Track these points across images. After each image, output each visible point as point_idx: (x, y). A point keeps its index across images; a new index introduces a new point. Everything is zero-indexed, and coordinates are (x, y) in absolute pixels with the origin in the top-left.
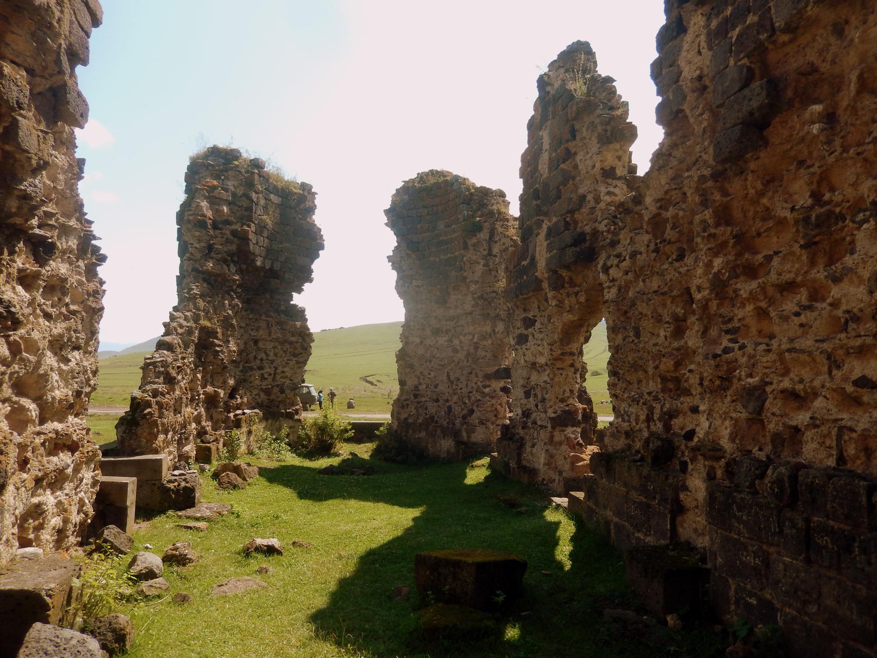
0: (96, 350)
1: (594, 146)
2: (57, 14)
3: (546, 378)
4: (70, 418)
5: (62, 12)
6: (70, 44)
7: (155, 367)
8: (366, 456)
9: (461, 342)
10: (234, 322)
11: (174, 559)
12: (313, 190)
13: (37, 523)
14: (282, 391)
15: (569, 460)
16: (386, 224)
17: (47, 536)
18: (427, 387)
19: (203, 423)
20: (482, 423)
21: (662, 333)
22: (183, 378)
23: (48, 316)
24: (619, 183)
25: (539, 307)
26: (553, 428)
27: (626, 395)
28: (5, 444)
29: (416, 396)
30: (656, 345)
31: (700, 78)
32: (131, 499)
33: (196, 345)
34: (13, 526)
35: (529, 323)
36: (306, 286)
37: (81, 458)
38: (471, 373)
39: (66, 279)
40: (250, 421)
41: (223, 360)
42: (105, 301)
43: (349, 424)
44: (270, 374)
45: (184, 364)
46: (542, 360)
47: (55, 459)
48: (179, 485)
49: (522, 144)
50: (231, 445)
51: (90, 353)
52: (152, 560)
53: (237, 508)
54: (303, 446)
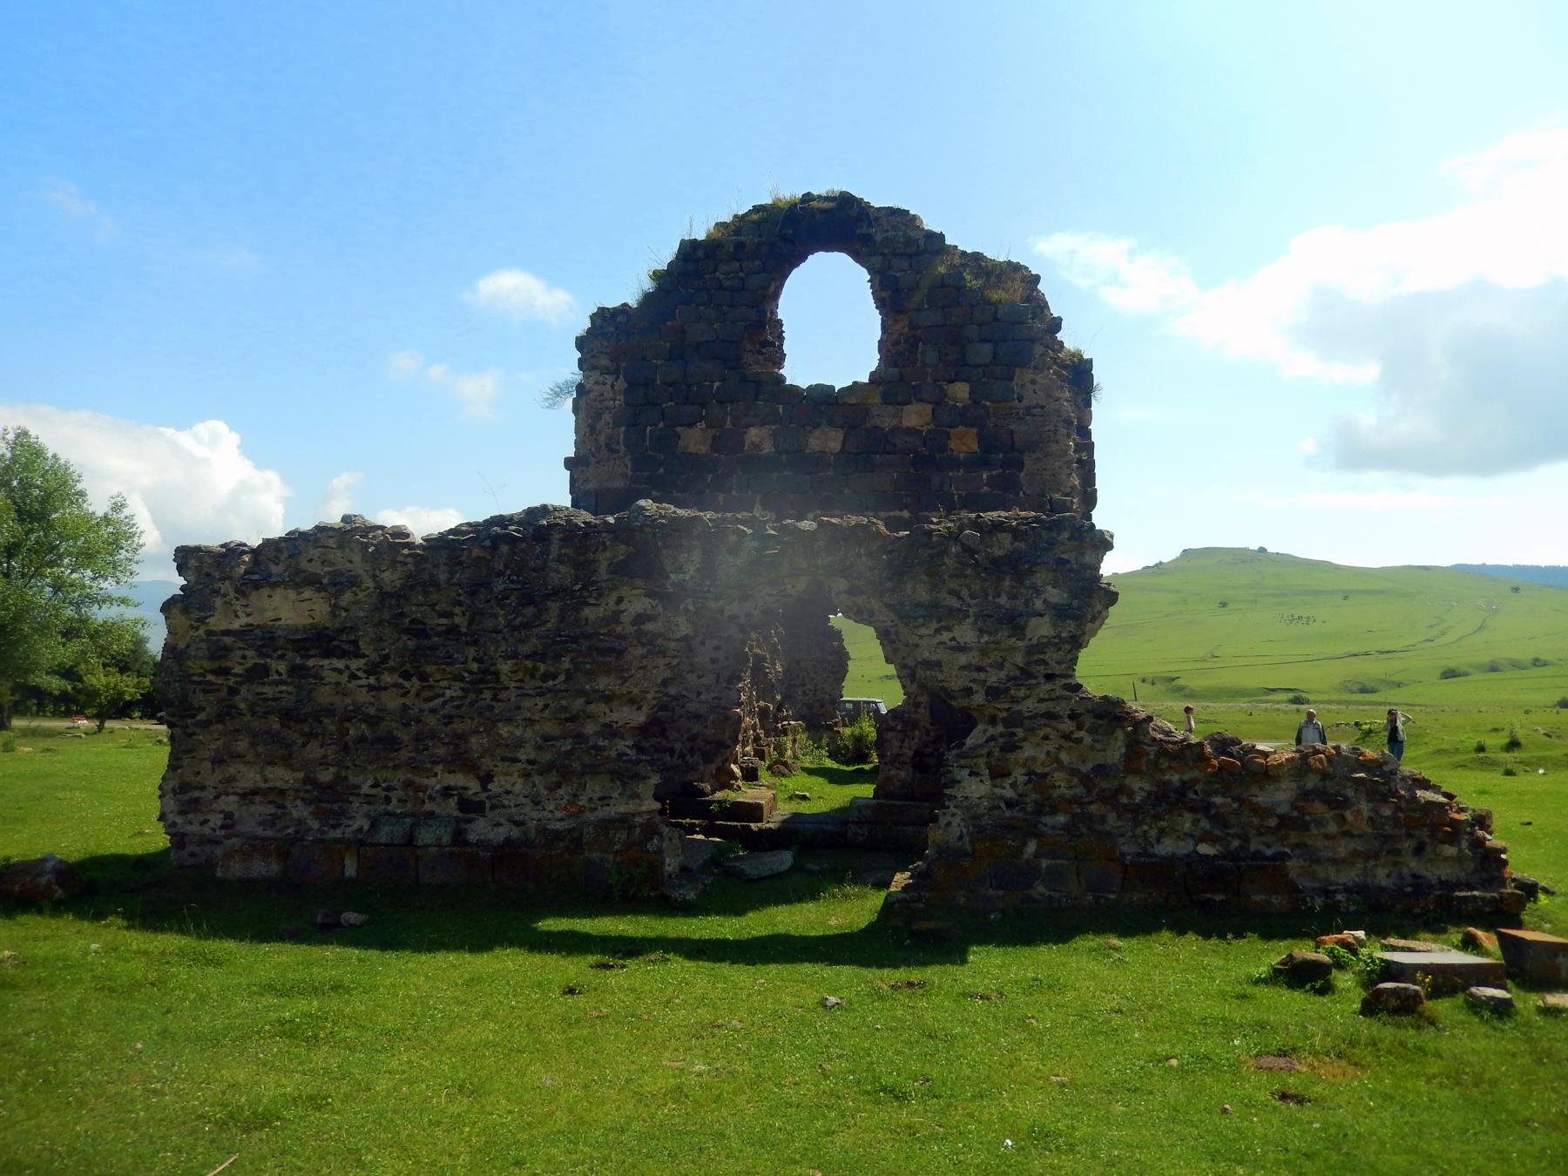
40: (795, 731)
50: (780, 749)
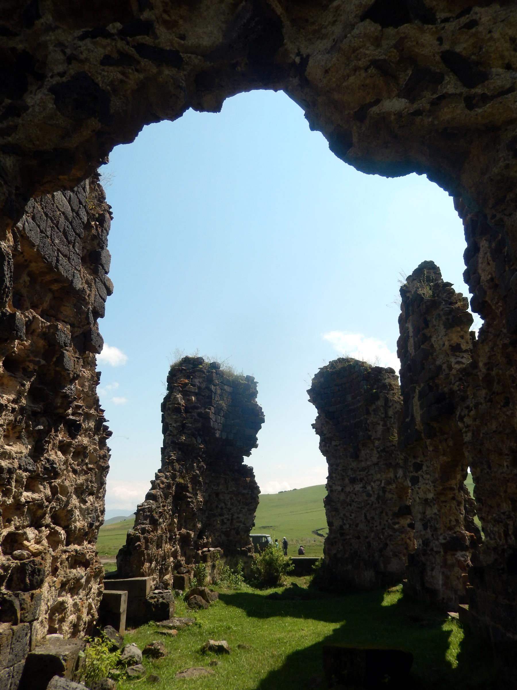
0: (104, 496)
1: (442, 330)
2: (88, 292)
3: (435, 511)
4: (85, 543)
5: (91, 291)
6: (95, 307)
7: (144, 512)
8: (305, 587)
9: (372, 487)
10: (201, 479)
11: (151, 653)
12: (255, 381)
13: (60, 616)
14: (238, 533)
15: (461, 580)
16: (309, 401)
17: (66, 627)
18: (350, 526)
19: (179, 558)
20: (395, 555)
21: (505, 464)
22: (164, 522)
23: (75, 472)
24: (465, 355)
25: (423, 454)
26: (445, 552)
27: (490, 517)
28: (45, 553)
29: (342, 534)
30: (502, 473)
31: (492, 279)
32: (123, 607)
33: (174, 497)
34: (46, 614)
35: (418, 467)
36: (253, 451)
37: (91, 572)
38: (382, 512)
39: (87, 447)
40: (214, 557)
41: (193, 508)
42: (110, 463)
43: (291, 559)
44: (228, 520)
45: (164, 510)
46: (430, 496)
47: (74, 571)
48: (158, 601)
49: (396, 334)
50: (200, 576)
51: (100, 498)
52: (134, 650)
53: (199, 621)
54: (255, 578)
